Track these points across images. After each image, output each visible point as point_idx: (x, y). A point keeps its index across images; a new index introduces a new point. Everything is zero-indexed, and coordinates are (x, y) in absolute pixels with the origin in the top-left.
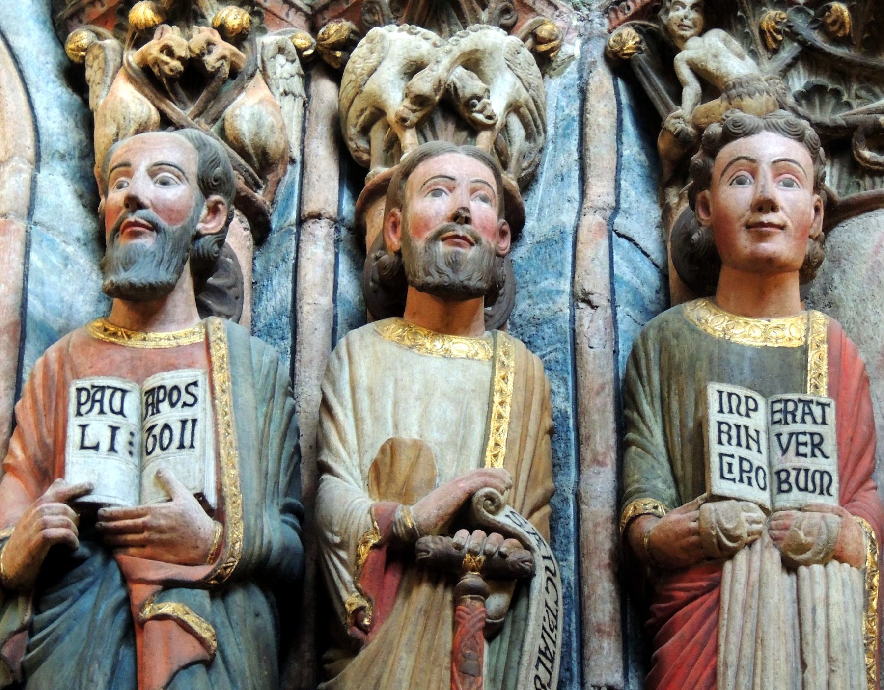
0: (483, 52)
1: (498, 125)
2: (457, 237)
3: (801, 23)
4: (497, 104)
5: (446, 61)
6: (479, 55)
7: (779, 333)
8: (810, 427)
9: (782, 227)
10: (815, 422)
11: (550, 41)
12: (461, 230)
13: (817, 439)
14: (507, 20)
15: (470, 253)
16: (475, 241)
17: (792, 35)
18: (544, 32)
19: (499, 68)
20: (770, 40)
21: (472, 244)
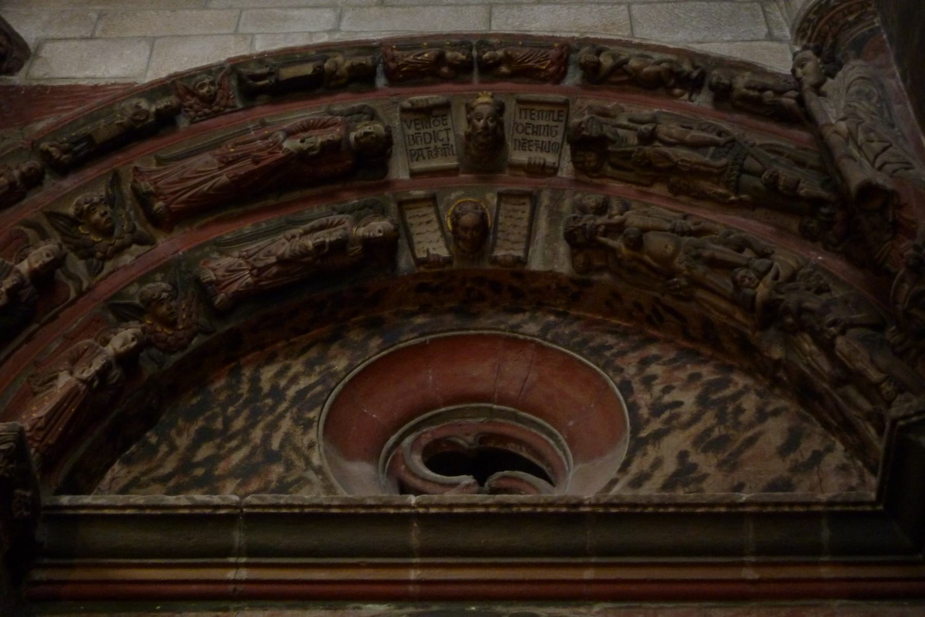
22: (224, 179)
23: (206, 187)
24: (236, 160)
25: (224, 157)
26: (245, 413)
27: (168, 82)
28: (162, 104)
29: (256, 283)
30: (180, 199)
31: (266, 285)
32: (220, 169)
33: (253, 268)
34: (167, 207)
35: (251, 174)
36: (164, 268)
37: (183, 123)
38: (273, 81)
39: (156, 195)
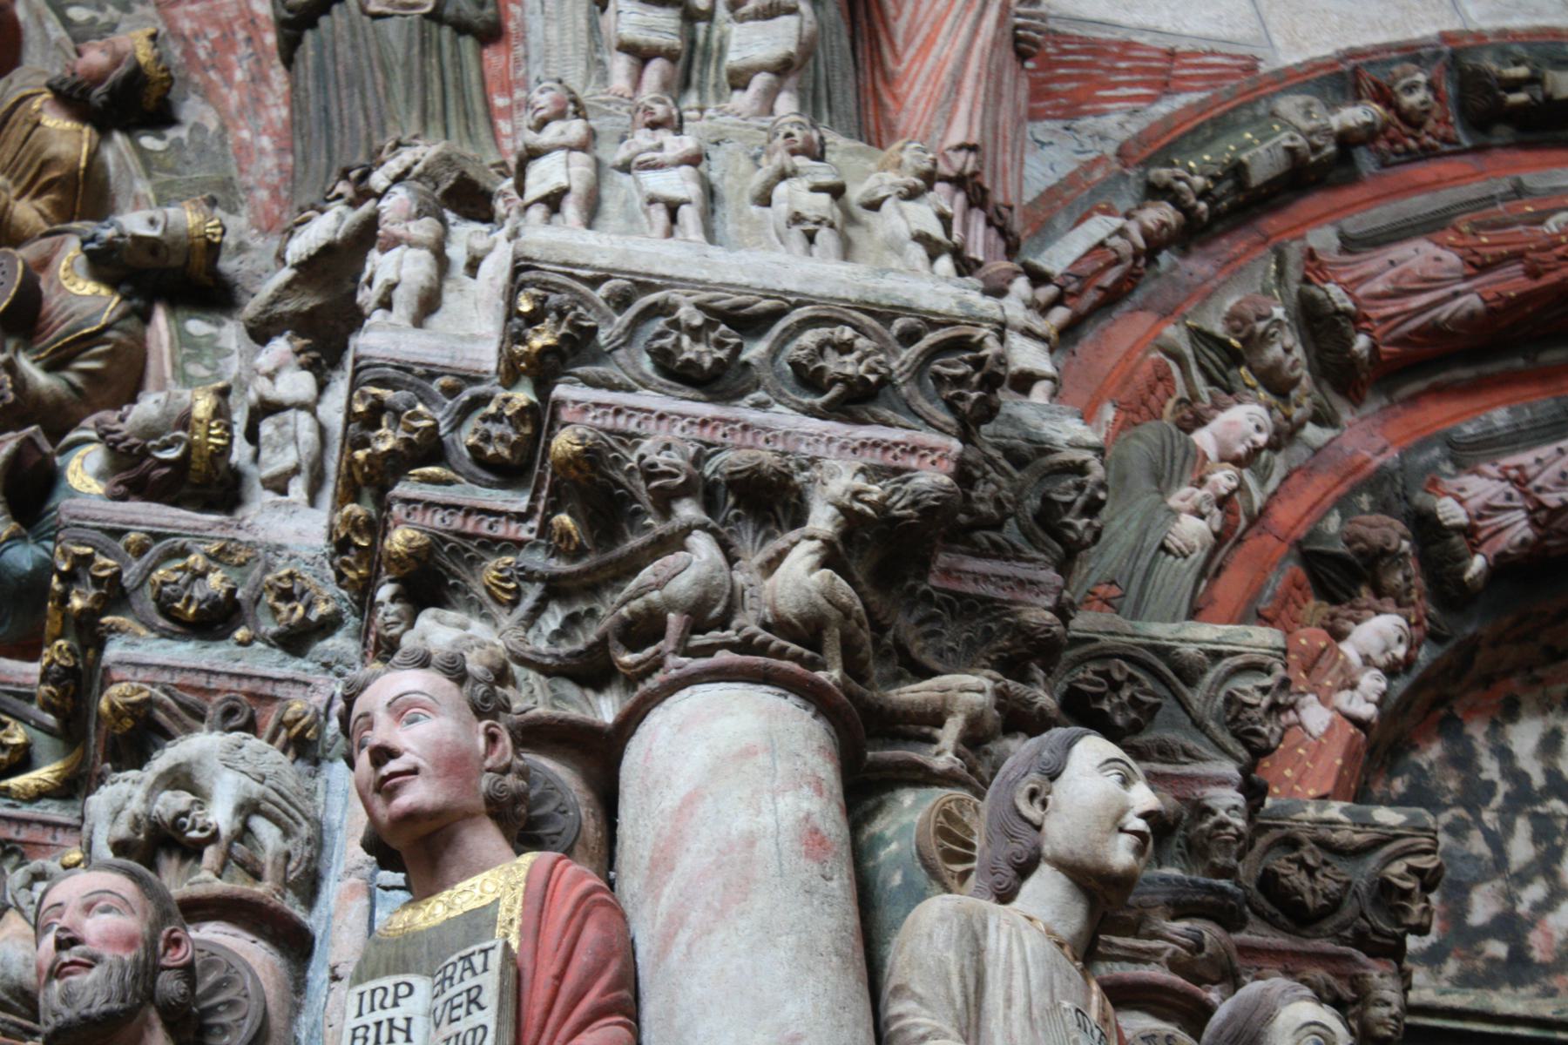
0: (188, 764)
1: (225, 831)
2: (65, 965)
3: (539, 561)
4: (221, 815)
5: (139, 792)
6: (184, 769)
7: (466, 896)
8: (470, 982)
9: (414, 771)
10: (475, 974)
11: (297, 720)
12: (66, 957)
13: (474, 993)
14: (239, 720)
15: (88, 977)
16: (91, 962)
17: (529, 576)
18: (289, 716)
19: (214, 773)
20: (499, 593)
21: (90, 966)
22: (1472, 302)
23: (1445, 312)
24: (1499, 262)
25: (1476, 254)
26: (1522, 826)
27: (1345, 67)
28: (1354, 115)
29: (1540, 539)
30: (1394, 334)
31: (1557, 547)
32: (1467, 278)
33: (1541, 506)
34: (1374, 348)
35: (1525, 298)
36: (1377, 482)
37: (1365, 160)
38: (1539, 97)
39: (1357, 319)
